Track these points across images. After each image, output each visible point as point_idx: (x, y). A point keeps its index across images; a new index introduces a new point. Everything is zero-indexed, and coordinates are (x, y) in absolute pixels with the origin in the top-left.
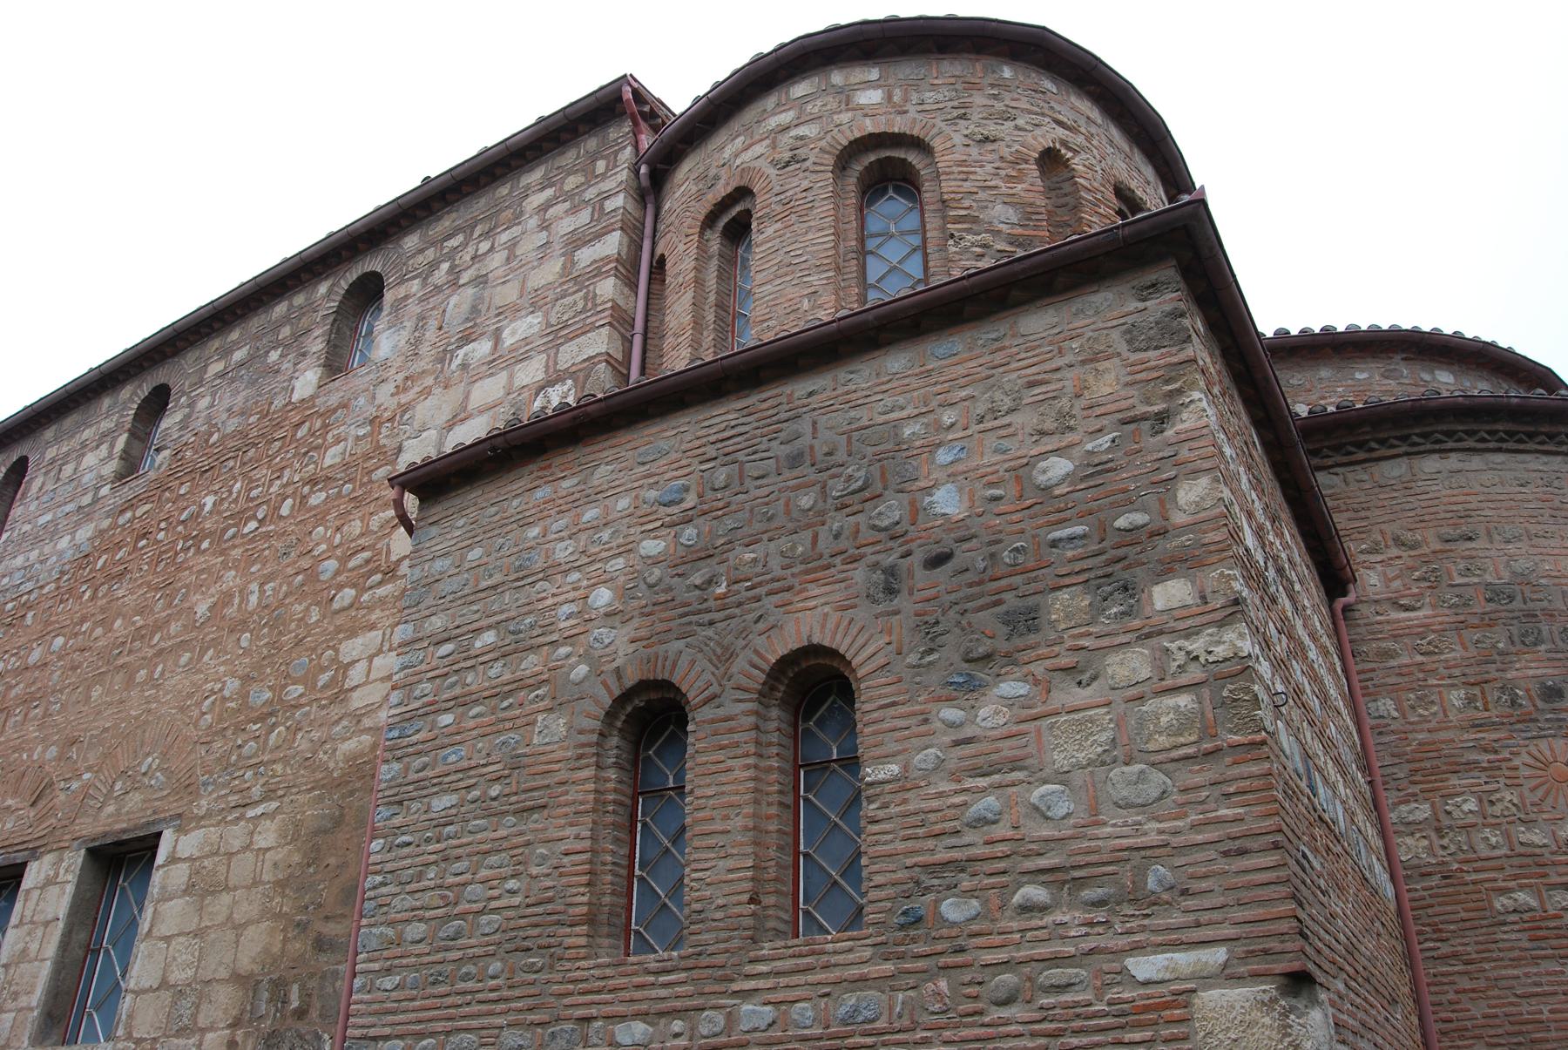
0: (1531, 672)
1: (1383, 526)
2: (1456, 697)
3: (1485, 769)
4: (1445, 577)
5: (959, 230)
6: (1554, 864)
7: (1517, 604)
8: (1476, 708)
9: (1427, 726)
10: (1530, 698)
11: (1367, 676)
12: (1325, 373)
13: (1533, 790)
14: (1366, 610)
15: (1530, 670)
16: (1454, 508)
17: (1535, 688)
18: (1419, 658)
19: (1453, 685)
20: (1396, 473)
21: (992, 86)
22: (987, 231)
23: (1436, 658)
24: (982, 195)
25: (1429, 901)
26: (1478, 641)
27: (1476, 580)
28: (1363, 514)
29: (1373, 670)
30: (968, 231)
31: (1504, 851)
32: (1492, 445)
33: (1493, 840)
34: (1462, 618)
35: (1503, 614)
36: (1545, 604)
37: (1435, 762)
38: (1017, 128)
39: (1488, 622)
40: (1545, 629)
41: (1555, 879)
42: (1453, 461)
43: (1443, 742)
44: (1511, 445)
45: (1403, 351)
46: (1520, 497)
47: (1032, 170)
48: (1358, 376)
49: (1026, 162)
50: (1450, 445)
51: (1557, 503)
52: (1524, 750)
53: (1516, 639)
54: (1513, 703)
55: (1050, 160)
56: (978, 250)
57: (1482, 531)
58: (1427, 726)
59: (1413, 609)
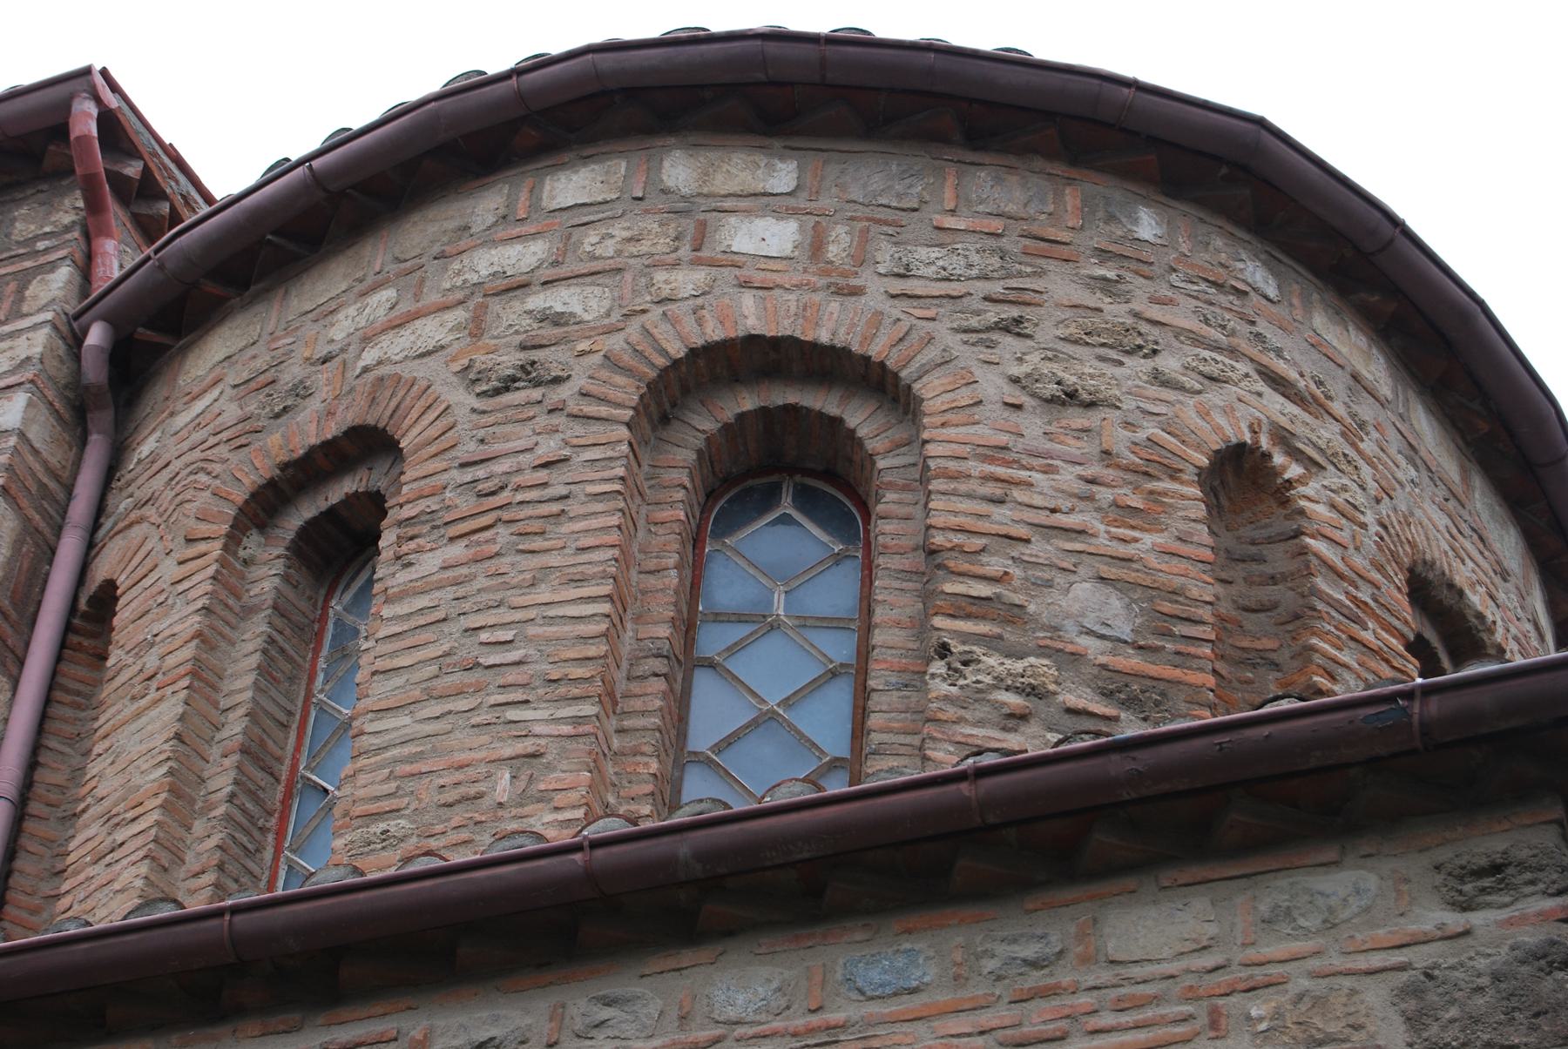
5: (965, 638)
21: (1103, 255)
22: (1043, 651)
24: (1041, 549)
38: (1158, 378)
47: (1188, 498)
49: (1174, 474)
55: (1240, 478)
56: (1013, 700)
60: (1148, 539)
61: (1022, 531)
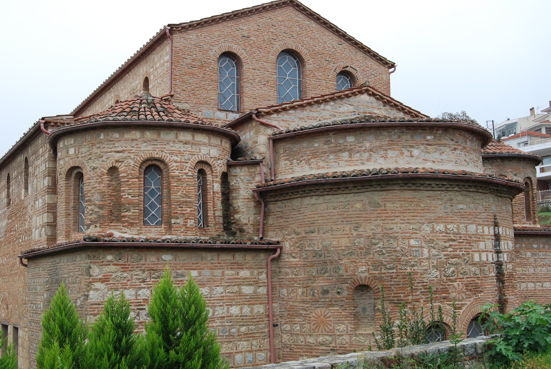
0: (320, 284)
1: (292, 225)
2: (300, 291)
3: (303, 316)
5: (87, 205)
6: (315, 349)
7: (322, 258)
9: (293, 300)
10: (318, 293)
11: (281, 280)
12: (305, 144)
13: (314, 325)
14: (285, 256)
15: (321, 283)
16: (310, 220)
17: (320, 290)
18: (294, 276)
19: (300, 287)
20: (297, 205)
21: (98, 143)
22: (93, 205)
25: (287, 355)
28: (288, 220)
30: (89, 205)
31: (303, 343)
33: (302, 339)
35: (316, 262)
38: (103, 161)
39: (312, 265)
40: (329, 267)
41: (314, 354)
42: (313, 200)
46: (333, 214)
48: (316, 145)
49: (104, 175)
50: (312, 194)
51: (345, 216)
53: (319, 271)
54: (313, 295)
55: (113, 170)
56: (90, 212)
58: (293, 300)
59: (294, 257)
60: (103, 185)
61: (91, 189)
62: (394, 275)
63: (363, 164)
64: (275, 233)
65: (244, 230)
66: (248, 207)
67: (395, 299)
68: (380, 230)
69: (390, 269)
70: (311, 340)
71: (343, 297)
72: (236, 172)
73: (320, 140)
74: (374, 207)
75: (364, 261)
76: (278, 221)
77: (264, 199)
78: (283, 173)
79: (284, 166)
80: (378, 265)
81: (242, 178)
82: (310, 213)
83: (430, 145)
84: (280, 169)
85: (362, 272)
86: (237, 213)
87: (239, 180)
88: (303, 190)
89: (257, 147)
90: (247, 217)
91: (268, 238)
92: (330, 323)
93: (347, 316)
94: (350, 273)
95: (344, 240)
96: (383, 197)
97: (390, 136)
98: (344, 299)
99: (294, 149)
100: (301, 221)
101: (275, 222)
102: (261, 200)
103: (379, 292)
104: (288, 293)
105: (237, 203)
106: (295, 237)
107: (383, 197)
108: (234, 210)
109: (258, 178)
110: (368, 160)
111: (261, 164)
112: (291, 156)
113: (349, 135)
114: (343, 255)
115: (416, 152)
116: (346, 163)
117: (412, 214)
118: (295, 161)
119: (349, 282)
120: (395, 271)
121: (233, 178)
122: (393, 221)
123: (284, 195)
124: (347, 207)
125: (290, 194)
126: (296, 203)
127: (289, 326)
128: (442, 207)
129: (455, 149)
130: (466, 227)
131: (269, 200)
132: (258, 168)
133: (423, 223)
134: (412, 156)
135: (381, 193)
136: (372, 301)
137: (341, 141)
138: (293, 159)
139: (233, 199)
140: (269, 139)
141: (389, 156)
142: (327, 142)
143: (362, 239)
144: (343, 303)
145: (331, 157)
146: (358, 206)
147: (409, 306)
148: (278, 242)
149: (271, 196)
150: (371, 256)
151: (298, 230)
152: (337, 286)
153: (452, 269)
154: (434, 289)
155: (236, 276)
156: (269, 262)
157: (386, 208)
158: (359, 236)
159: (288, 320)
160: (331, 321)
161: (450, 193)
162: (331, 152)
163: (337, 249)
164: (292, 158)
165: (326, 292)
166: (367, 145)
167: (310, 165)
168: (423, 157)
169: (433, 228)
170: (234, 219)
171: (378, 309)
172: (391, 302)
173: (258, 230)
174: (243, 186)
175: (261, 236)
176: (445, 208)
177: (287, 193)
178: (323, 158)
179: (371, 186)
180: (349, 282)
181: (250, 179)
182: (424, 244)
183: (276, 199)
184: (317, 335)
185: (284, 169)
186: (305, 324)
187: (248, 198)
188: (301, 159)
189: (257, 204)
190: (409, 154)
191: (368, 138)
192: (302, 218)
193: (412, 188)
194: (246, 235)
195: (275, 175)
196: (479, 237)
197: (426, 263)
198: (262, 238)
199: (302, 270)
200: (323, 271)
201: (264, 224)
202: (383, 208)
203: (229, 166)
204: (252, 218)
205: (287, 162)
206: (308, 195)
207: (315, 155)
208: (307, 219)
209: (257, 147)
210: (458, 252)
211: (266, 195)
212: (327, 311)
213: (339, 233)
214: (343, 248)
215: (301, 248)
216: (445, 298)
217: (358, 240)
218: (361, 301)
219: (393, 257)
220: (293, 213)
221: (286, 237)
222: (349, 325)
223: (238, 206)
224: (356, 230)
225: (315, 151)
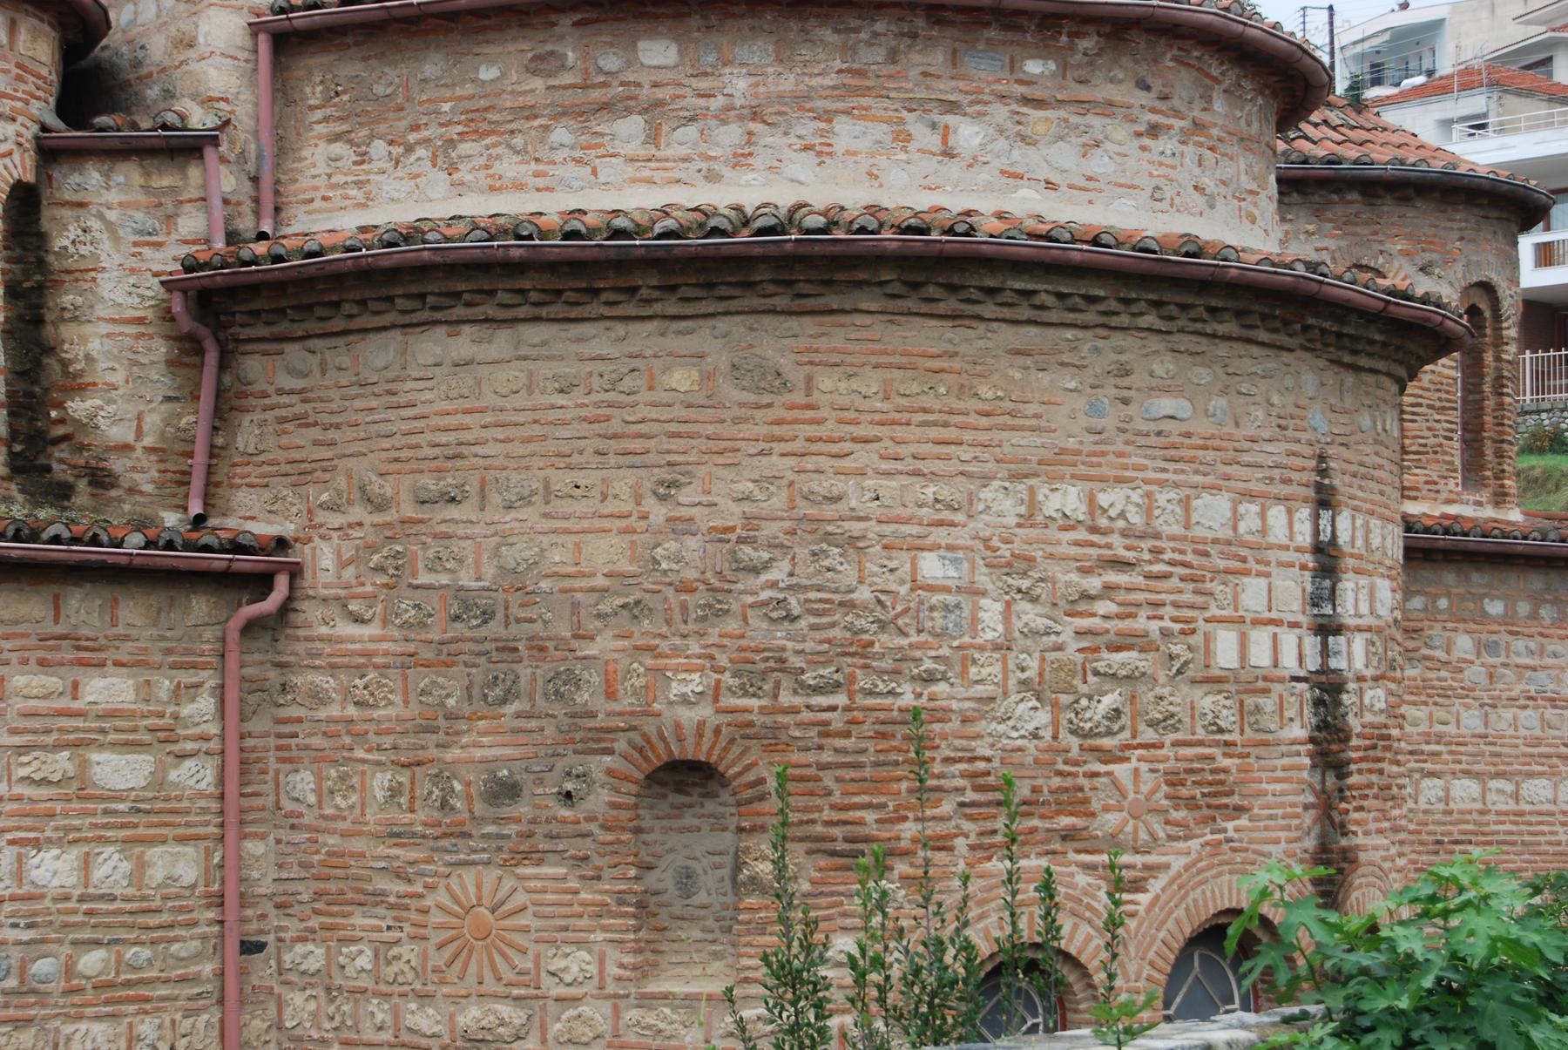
0: (478, 753)
1: (352, 463)
2: (380, 782)
3: (391, 907)
4: (408, 571)
7: (495, 628)
8: (400, 805)
9: (342, 825)
10: (469, 797)
11: (287, 729)
12: (432, 66)
13: (441, 946)
14: (310, 613)
15: (483, 748)
16: (443, 438)
17: (478, 779)
18: (351, 711)
19: (378, 763)
20: (380, 363)
23: (368, 713)
26: (423, 692)
27: (444, 579)
28: (332, 434)
29: (299, 720)
32: (522, 312)
33: (380, 1017)
34: (411, 647)
36: (537, 628)
37: (342, 885)
40: (525, 672)
42: (464, 344)
43: (352, 855)
44: (558, 309)
45: (574, 8)
46: (553, 415)
48: (487, 73)
50: (460, 311)
51: (615, 426)
52: (443, 882)
53: (476, 691)
54: (444, 805)
57: (472, 488)
58: (342, 825)
59: (358, 620)
62: (837, 720)
63: (712, 177)
64: (267, 495)
65: (110, 474)
66: (136, 363)
67: (837, 832)
68: (778, 502)
69: (817, 690)
70: (425, 1020)
71: (589, 819)
72: (80, 188)
73: (511, 47)
74: (758, 390)
75: (695, 648)
76: (284, 440)
77: (218, 328)
78: (318, 204)
79: (322, 169)
80: (762, 668)
81: (112, 215)
82: (445, 405)
83: (1039, 103)
84: (305, 182)
85: (685, 700)
86: (77, 386)
87: (95, 224)
88: (414, 289)
89: (194, 66)
90: (131, 410)
91: (231, 522)
92: (518, 938)
93: (601, 911)
94: (626, 703)
95: (603, 542)
96: (803, 342)
97: (849, 50)
98: (593, 827)
99: (380, 89)
100: (398, 441)
101: (270, 441)
102: (203, 332)
103: (762, 798)
104: (318, 791)
105: (84, 340)
106: (368, 519)
107: (803, 342)
108: (66, 373)
109: (191, 223)
110: (740, 160)
111: (209, 153)
112: (360, 121)
113: (653, 35)
114: (599, 616)
115: (968, 134)
116: (630, 171)
117: (934, 433)
118: (379, 148)
119: (621, 745)
120: (840, 699)
121: (66, 213)
122: (846, 463)
123: (319, 312)
124: (625, 385)
125: (348, 308)
126: (379, 353)
127: (320, 951)
128: (1080, 403)
129: (1154, 131)
130: (1186, 503)
131: (244, 333)
132: (194, 172)
133: (986, 479)
134: (949, 154)
135: (793, 323)
136: (727, 840)
137: (610, 62)
138: (372, 137)
139: (63, 320)
140: (255, 29)
141: (841, 143)
142: (541, 64)
143: (692, 543)
144: (586, 847)
145: (560, 135)
146: (682, 379)
147: (901, 867)
148: (282, 544)
149: (255, 314)
150: (732, 626)
151: (377, 486)
152: (561, 764)
153: (1109, 701)
154: (1023, 790)
155: (65, 703)
156: (234, 636)
157: (816, 397)
158: (680, 527)
159: (314, 923)
160: (525, 930)
161: (1118, 339)
162: (563, 113)
163: (567, 583)
164: (364, 132)
165: (506, 791)
166: (739, 85)
167: (452, 169)
168: (1002, 163)
169: (1033, 503)
170: (61, 421)
171: (753, 879)
172: (818, 845)
173: (183, 479)
174: (117, 259)
175: (196, 508)
176: (1094, 409)
177: (337, 305)
178: (518, 141)
179: (749, 285)
180: (621, 745)
181: (151, 223)
182: (983, 579)
183: (276, 329)
184: (455, 999)
185: (321, 182)
186: (397, 942)
187: (139, 321)
188: (412, 137)
189: (183, 351)
190: (934, 141)
191: (741, 52)
192: (405, 426)
193: (941, 308)
194: (120, 500)
195: (277, 210)
196: (1244, 556)
197: (988, 668)
198: (199, 520)
199: (393, 680)
200: (498, 692)
201: (213, 452)
202: (799, 397)
203: (49, 153)
204: (153, 420)
205: (338, 148)
206: (438, 315)
207: (480, 122)
208: (429, 436)
209: (194, 66)
210: (1141, 623)
211: (236, 310)
212: (508, 884)
213: (581, 507)
214: (600, 582)
215: (396, 575)
216: (1068, 836)
217: (672, 546)
218: (674, 840)
219: (835, 633)
220: (359, 404)
221: (321, 517)
222: (613, 954)
223: (89, 359)
224: (662, 499)
225: (483, 103)
